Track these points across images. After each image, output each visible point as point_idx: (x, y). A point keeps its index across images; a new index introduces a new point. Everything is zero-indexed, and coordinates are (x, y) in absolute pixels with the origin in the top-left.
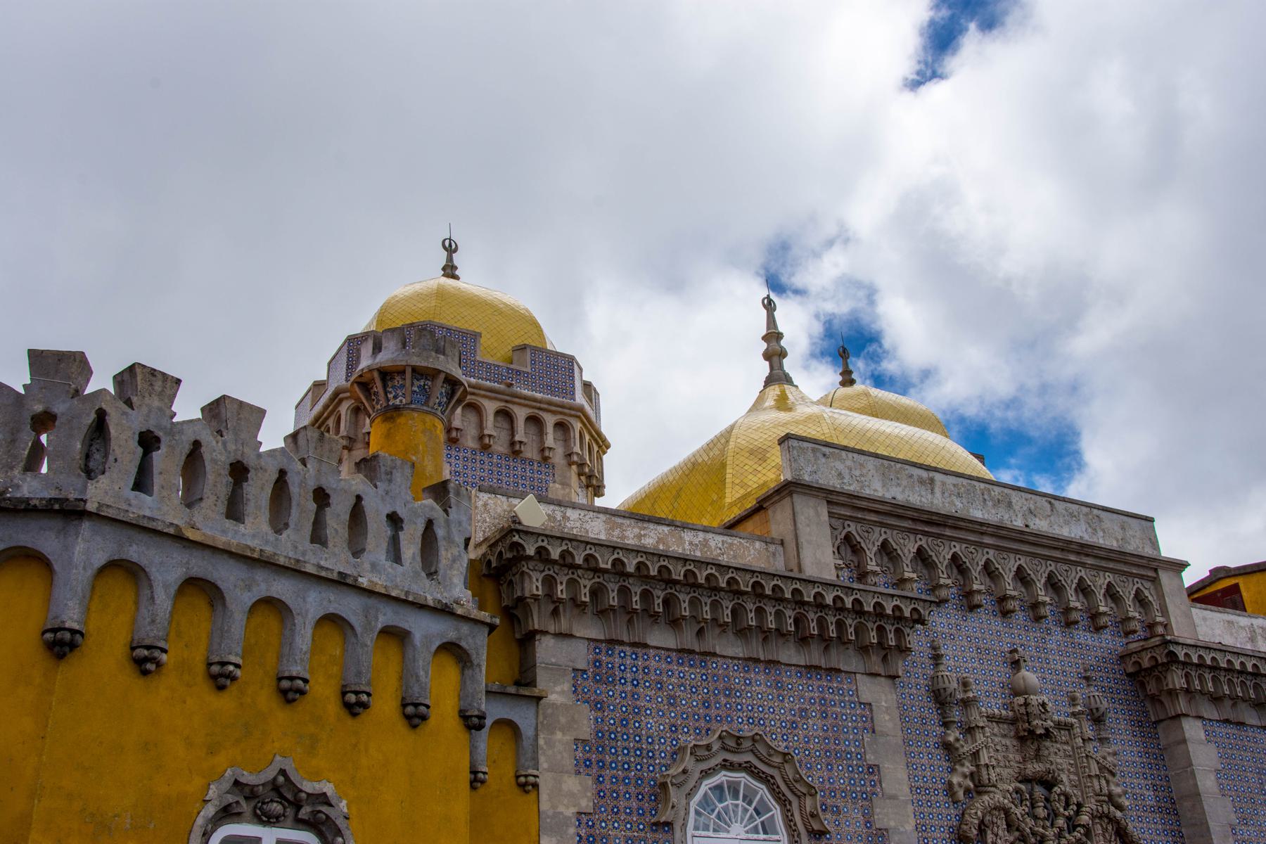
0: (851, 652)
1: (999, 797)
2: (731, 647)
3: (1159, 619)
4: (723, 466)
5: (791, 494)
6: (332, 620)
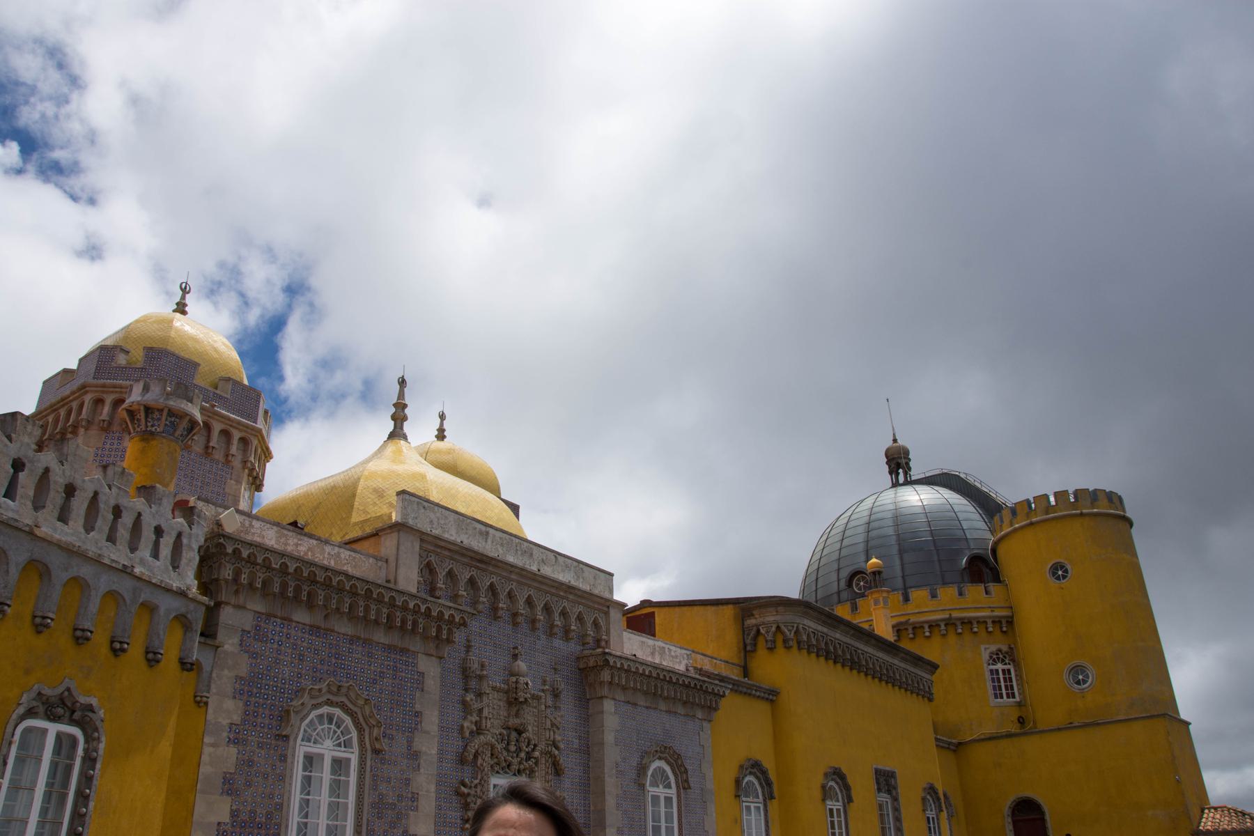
0: (418, 638)
1: (488, 738)
2: (344, 628)
4: (354, 495)
6: (112, 595)
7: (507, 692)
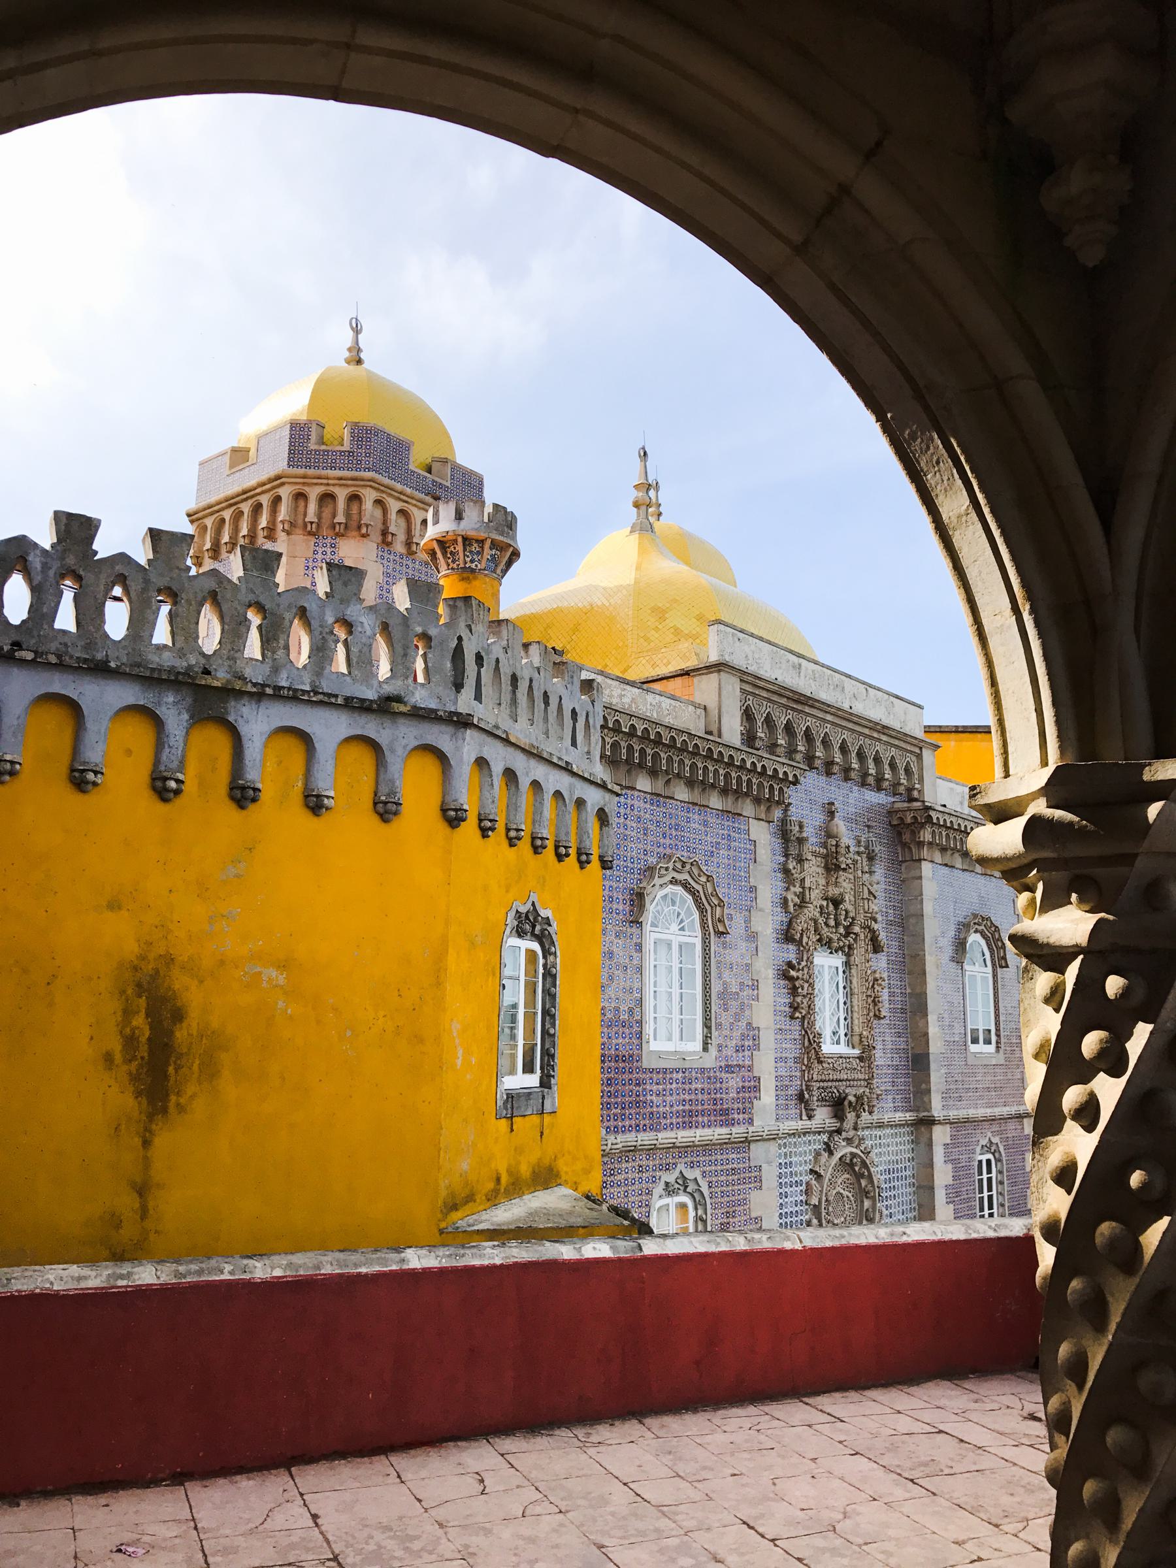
2: (682, 793)
3: (917, 786)
5: (719, 671)
7: (825, 857)
